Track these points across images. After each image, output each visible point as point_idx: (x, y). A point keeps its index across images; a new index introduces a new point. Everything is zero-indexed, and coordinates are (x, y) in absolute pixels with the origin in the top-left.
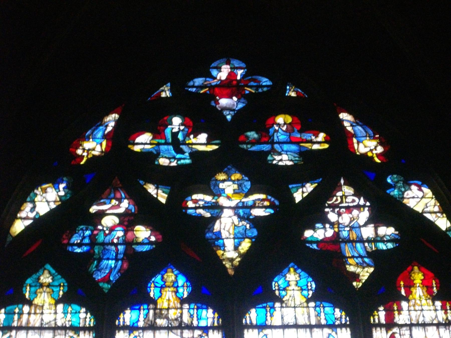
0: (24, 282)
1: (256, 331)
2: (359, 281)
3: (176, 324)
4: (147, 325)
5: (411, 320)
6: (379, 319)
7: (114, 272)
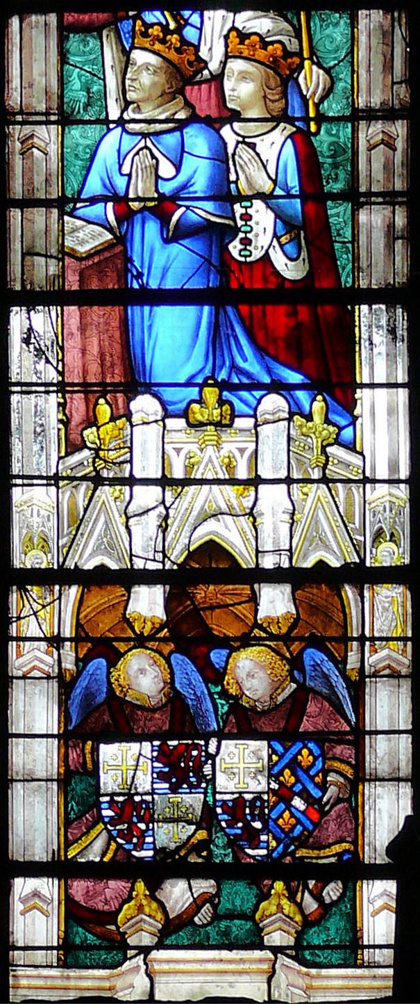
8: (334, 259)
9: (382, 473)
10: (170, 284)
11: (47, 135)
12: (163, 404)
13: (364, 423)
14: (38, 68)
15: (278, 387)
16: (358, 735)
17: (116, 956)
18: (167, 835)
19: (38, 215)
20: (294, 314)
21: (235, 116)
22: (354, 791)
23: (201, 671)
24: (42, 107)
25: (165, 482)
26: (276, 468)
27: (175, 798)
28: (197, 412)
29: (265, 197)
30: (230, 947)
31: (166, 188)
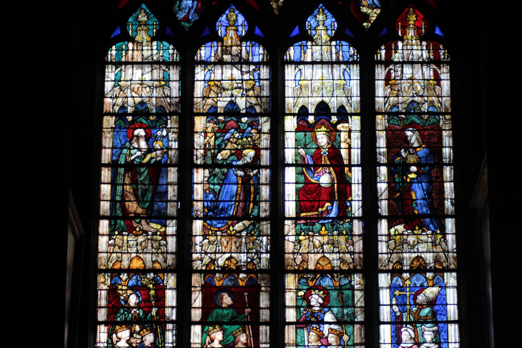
0: (127, 21)
1: (293, 66)
2: (369, 22)
3: (237, 60)
4: (217, 61)
5: (403, 58)
6: (380, 56)
7: (192, 12)
24: (292, 343)
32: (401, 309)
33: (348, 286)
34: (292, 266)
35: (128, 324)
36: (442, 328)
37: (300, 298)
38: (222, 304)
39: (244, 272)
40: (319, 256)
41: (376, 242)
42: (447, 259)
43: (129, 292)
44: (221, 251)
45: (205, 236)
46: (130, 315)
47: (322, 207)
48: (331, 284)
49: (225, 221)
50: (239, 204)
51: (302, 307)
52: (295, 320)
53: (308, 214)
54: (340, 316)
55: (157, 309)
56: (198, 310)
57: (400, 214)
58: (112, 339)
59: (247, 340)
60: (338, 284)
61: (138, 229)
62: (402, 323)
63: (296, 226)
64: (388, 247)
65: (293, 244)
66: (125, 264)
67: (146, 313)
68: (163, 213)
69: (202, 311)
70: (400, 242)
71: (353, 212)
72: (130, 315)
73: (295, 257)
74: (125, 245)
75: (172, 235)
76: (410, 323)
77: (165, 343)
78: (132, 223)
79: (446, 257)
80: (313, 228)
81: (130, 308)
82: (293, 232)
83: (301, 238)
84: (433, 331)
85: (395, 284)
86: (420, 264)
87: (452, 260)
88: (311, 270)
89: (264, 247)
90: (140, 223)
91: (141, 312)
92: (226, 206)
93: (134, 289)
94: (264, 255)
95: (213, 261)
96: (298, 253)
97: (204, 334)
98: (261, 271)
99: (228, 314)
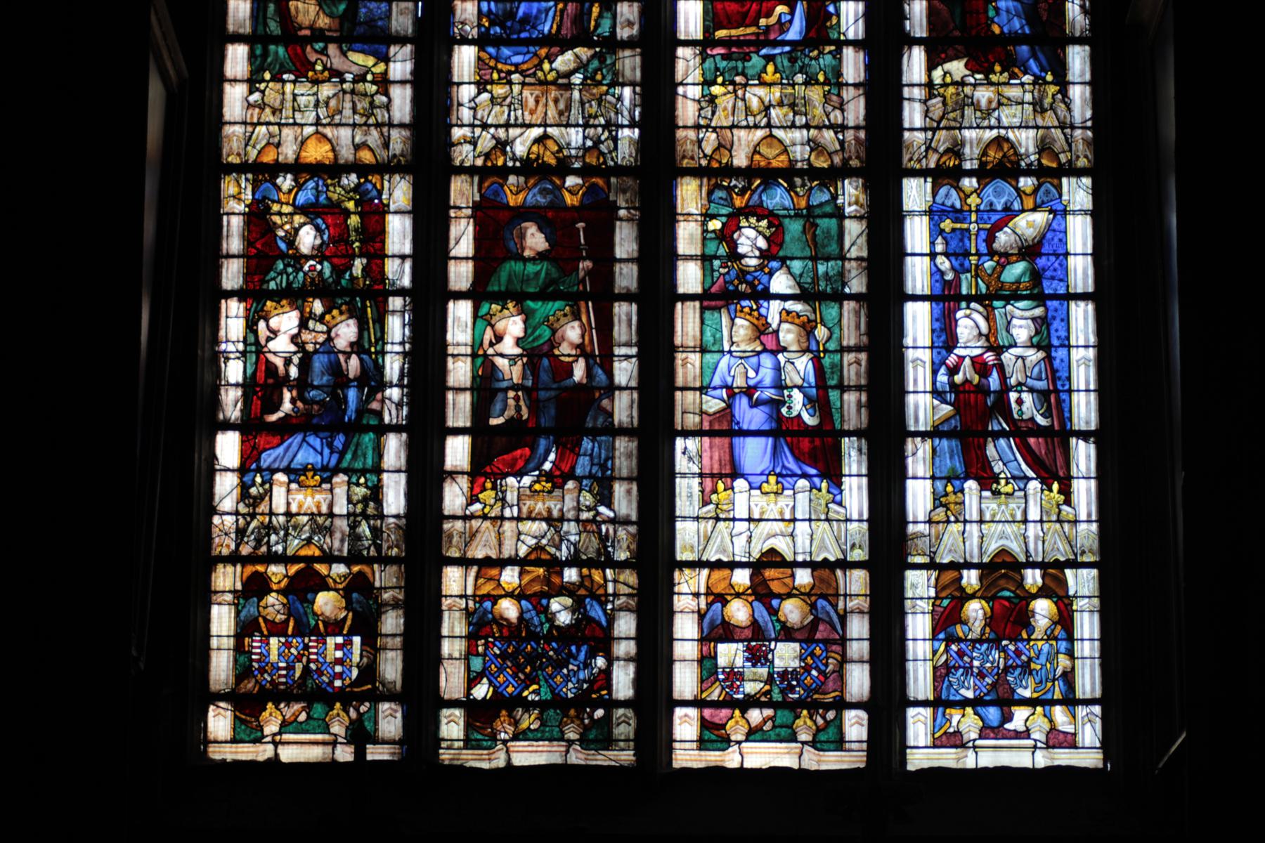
8: (832, 416)
9: (855, 516)
10: (753, 427)
11: (695, 358)
12: (750, 483)
13: (846, 493)
14: (690, 326)
15: (805, 476)
16: (843, 641)
17: (724, 745)
18: (750, 688)
19: (690, 396)
20: (812, 442)
21: (784, 349)
22: (841, 667)
23: (767, 610)
24: (691, 344)
25: (750, 520)
26: (803, 513)
27: (754, 670)
28: (766, 487)
29: (800, 388)
30: (781, 741)
31: (751, 383)
32: (956, 264)
33: (828, 209)
34: (692, 158)
35: (294, 296)
36: (1056, 310)
37: (713, 235)
38: (523, 249)
39: (576, 172)
40: (760, 133)
41: (897, 102)
42: (1070, 145)
43: (298, 219)
44: (520, 121)
45: (481, 85)
46: (301, 274)
47: (768, 15)
48: (788, 203)
49: (532, 49)
50: (565, 6)
51: (716, 257)
52: (699, 290)
53: (734, 32)
54: (809, 280)
55: (365, 261)
56: (464, 263)
57: (957, 33)
58: (256, 333)
59: (583, 336)
60: (803, 203)
61: (319, 68)
62: (959, 298)
63: (703, 61)
64: (926, 113)
65: (697, 106)
66: (289, 152)
67: (338, 271)
68: (381, 28)
69: (475, 266)
70: (957, 103)
71: (843, 29)
72: (301, 274)
73: (701, 136)
74: (289, 104)
75: (403, 82)
76: (979, 298)
77: (384, 343)
78: (304, 51)
79: (1067, 139)
80: (744, 68)
81: (299, 259)
82: (696, 76)
83: (716, 90)
84: (1034, 319)
85: (943, 204)
86: (1004, 156)
87: (1081, 147)
88: (739, 168)
89: (626, 113)
90: (323, 52)
91: (327, 269)
92: (535, 11)
93: (310, 211)
94: (626, 132)
95: (502, 145)
96: (707, 127)
97: (480, 323)
98: (619, 170)
99: (537, 274)
